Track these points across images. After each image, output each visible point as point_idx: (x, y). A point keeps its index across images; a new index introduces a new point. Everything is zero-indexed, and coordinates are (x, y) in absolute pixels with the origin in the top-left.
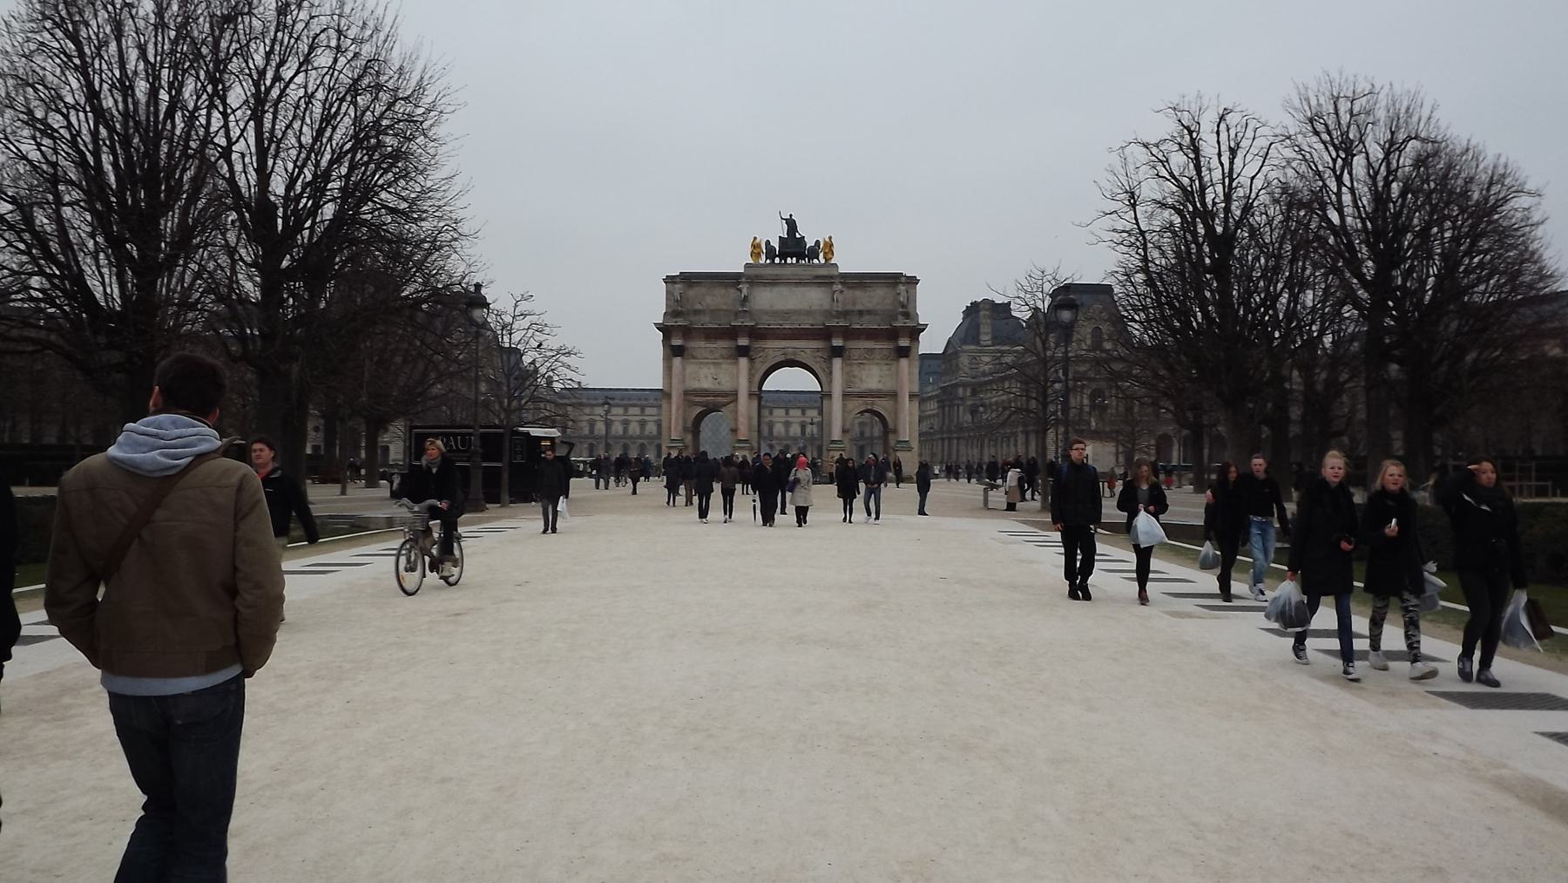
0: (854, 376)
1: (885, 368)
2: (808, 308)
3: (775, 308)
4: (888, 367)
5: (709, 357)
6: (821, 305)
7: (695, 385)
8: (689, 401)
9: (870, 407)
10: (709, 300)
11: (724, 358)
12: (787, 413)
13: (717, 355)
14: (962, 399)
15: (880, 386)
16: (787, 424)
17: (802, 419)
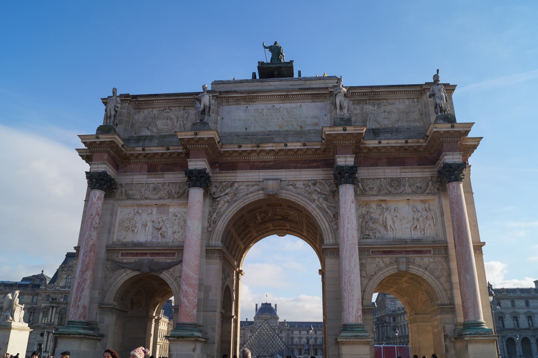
0: (374, 221)
1: (420, 206)
2: (299, 129)
3: (252, 129)
4: (427, 205)
5: (150, 197)
6: (316, 124)
7: (129, 238)
8: (114, 261)
9: (403, 267)
10: (160, 124)
11: (173, 198)
12: (300, 333)
13: (162, 193)
14: (389, 323)
15: (417, 235)
16: (300, 338)
17: (307, 336)
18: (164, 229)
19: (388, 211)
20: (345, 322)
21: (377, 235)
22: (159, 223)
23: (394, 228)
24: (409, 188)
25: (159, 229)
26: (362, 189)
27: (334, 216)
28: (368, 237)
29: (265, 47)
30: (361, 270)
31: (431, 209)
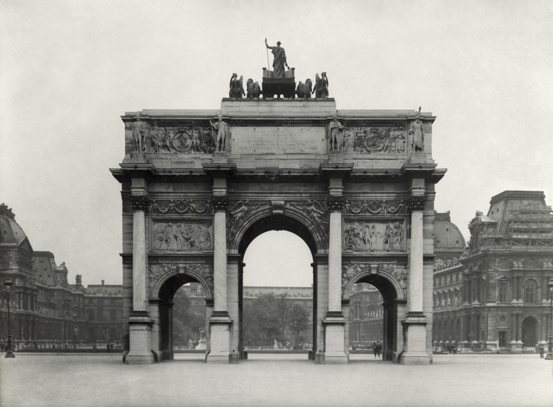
9: (374, 272)
18: (192, 240)
19: (367, 228)
20: (330, 310)
21: (357, 247)
22: (188, 234)
23: (370, 242)
24: (385, 210)
25: (186, 239)
26: (348, 209)
27: (326, 230)
28: (350, 248)
29: (268, 47)
30: (342, 274)
31: (400, 227)
